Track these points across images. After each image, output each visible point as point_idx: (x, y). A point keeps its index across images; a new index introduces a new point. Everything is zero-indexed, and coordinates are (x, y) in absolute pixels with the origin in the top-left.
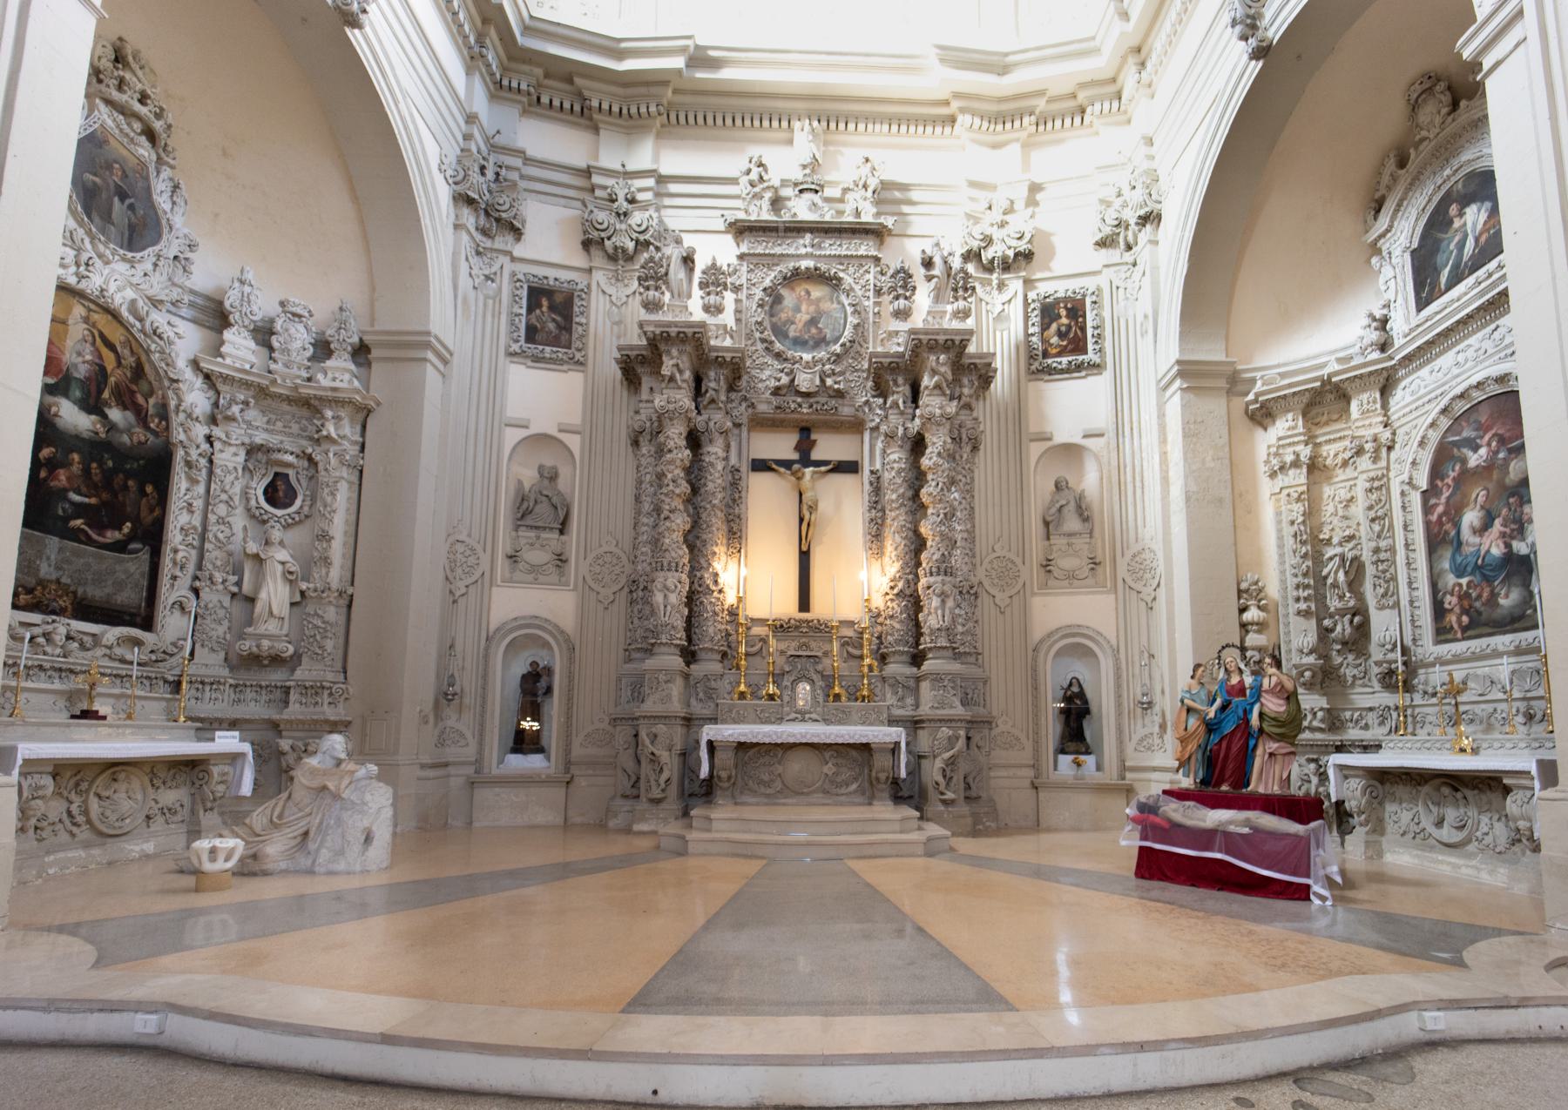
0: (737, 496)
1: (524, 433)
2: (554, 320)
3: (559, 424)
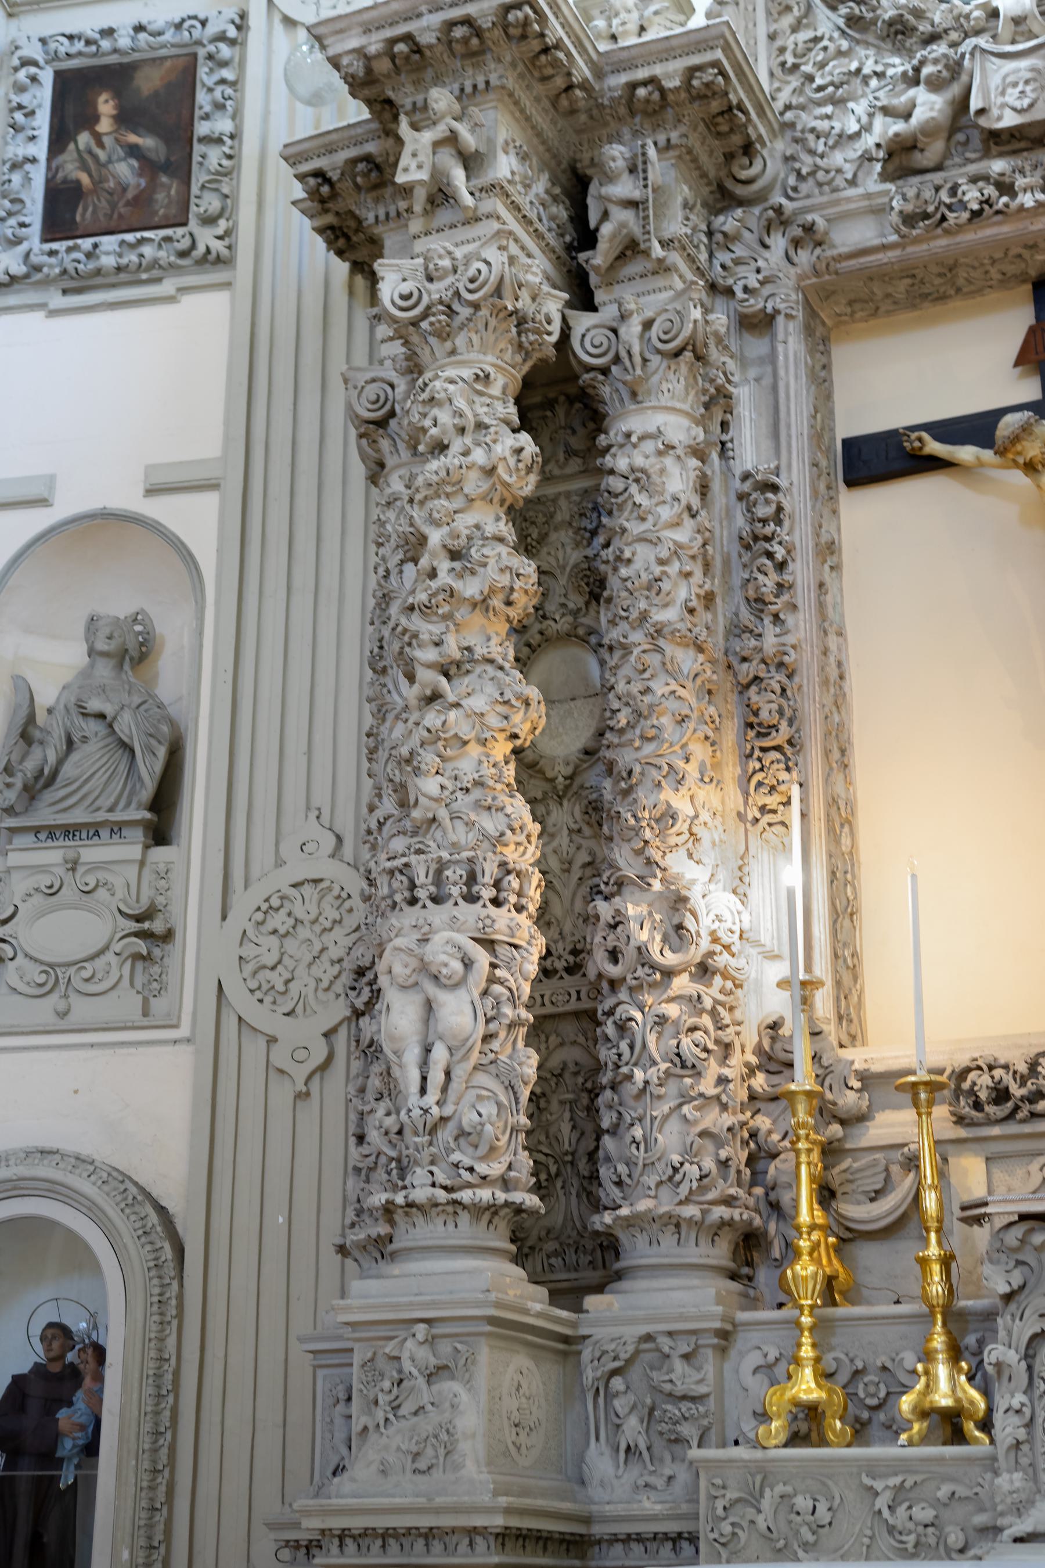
0: (768, 582)
1: (38, 521)
2: (133, 151)
3: (149, 469)
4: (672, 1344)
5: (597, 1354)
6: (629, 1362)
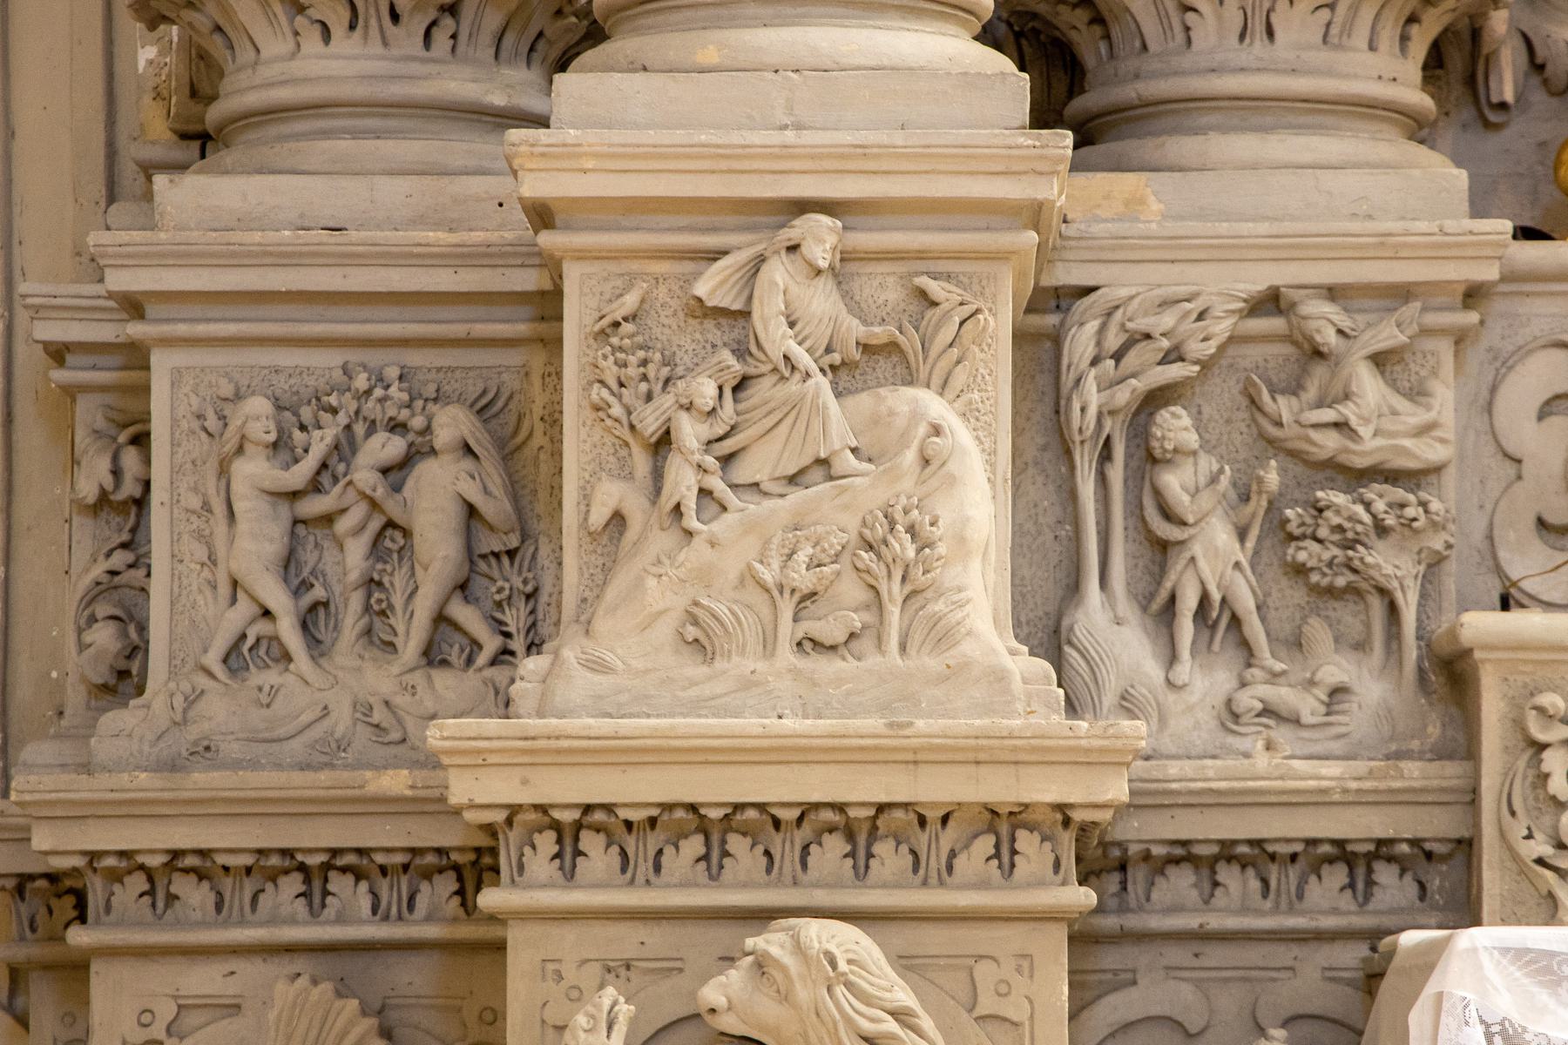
4: (1345, 323)
5: (1113, 341)
6: (1206, 365)
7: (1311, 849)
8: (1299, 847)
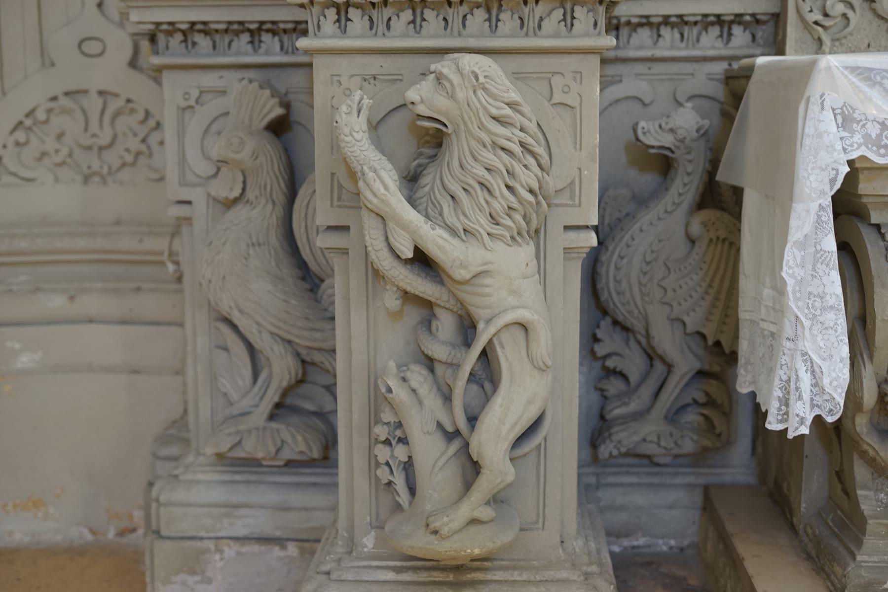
7: (705, 19)
8: (699, 18)
